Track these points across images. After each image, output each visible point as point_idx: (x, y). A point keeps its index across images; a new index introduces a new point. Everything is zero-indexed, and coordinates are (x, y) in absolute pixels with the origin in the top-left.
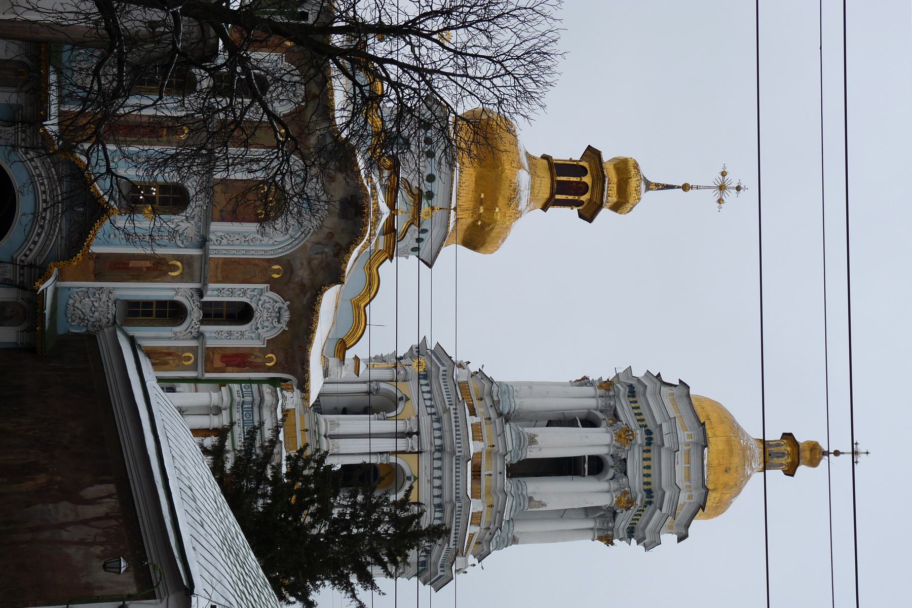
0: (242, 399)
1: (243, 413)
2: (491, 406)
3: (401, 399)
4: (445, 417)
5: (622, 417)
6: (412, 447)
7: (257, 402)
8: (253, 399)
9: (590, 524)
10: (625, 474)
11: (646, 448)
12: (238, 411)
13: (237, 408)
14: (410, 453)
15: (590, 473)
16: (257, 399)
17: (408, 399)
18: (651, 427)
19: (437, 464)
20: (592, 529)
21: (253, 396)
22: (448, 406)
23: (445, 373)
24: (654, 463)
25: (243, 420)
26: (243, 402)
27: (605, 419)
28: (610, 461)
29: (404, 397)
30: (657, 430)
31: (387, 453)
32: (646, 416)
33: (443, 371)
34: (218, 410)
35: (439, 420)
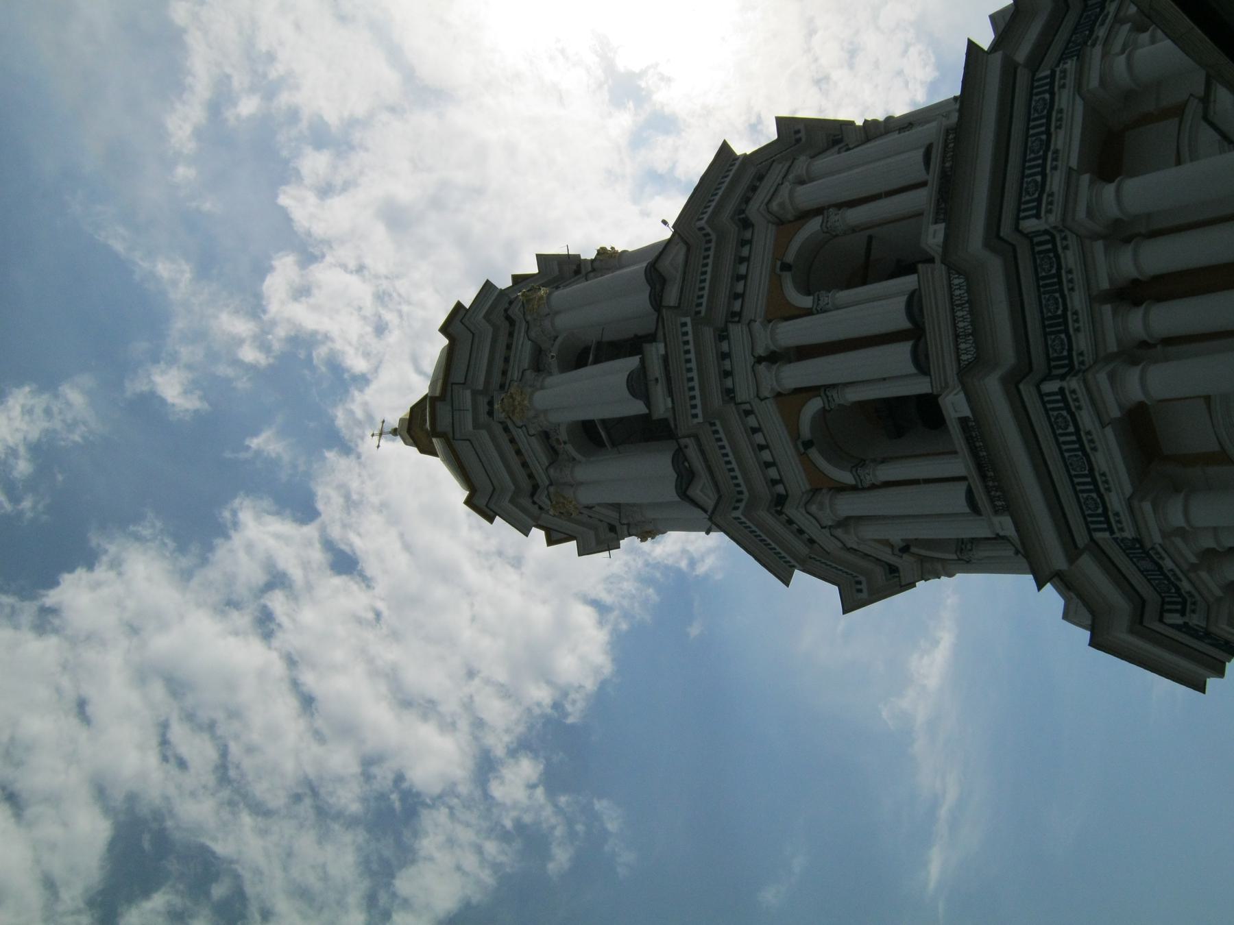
0: (1064, 384)
1: (1070, 350)
2: (686, 447)
3: (808, 444)
4: (717, 400)
5: (534, 440)
8: (1038, 387)
12: (1081, 354)
13: (1082, 363)
17: (796, 446)
21: (1041, 395)
22: (719, 427)
23: (737, 505)
25: (1067, 332)
26: (1062, 377)
27: (565, 443)
29: (802, 450)
31: (818, 313)
32: (509, 450)
33: (736, 508)
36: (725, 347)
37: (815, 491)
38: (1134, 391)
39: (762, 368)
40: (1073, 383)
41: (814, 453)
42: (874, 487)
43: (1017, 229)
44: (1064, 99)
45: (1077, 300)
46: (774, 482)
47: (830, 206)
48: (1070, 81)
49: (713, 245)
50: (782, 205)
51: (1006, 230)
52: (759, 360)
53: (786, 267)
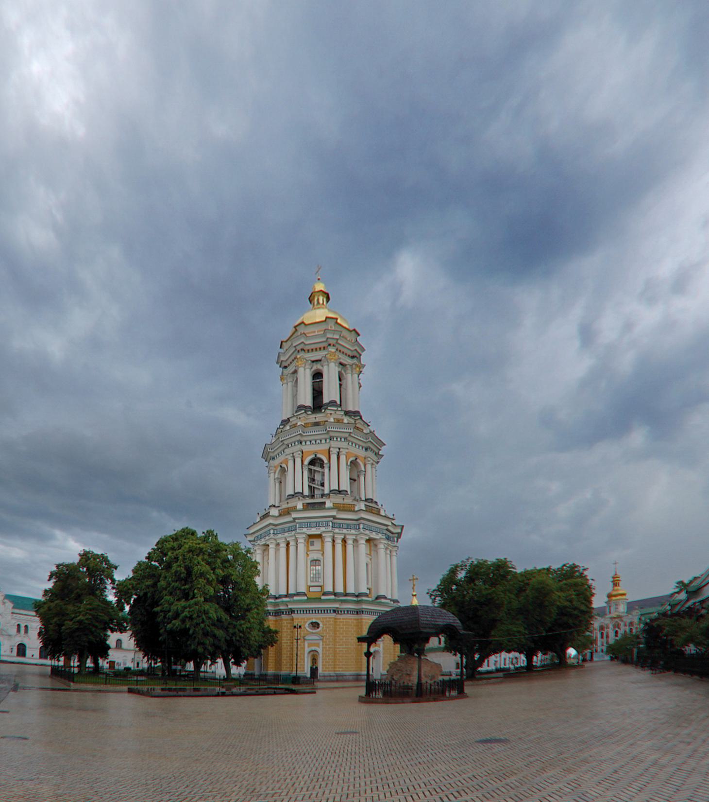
0: (272, 534)
3: (281, 466)
6: (299, 454)
7: (273, 527)
8: (272, 529)
9: (349, 375)
10: (320, 360)
11: (306, 351)
14: (302, 456)
15: (322, 378)
16: (271, 527)
17: (281, 463)
18: (296, 352)
19: (308, 443)
20: (352, 375)
24: (313, 347)
26: (273, 534)
28: (314, 368)
30: (297, 347)
34: (278, 545)
35: (288, 446)
36: (296, 443)
37: (275, 467)
38: (270, 546)
39: (292, 455)
40: (272, 536)
41: (279, 468)
42: (275, 482)
43: (297, 523)
44: (323, 529)
45: (286, 534)
46: (276, 457)
47: (330, 464)
48: (327, 530)
49: (325, 432)
50: (332, 451)
51: (297, 521)
52: (293, 454)
53: (316, 455)
